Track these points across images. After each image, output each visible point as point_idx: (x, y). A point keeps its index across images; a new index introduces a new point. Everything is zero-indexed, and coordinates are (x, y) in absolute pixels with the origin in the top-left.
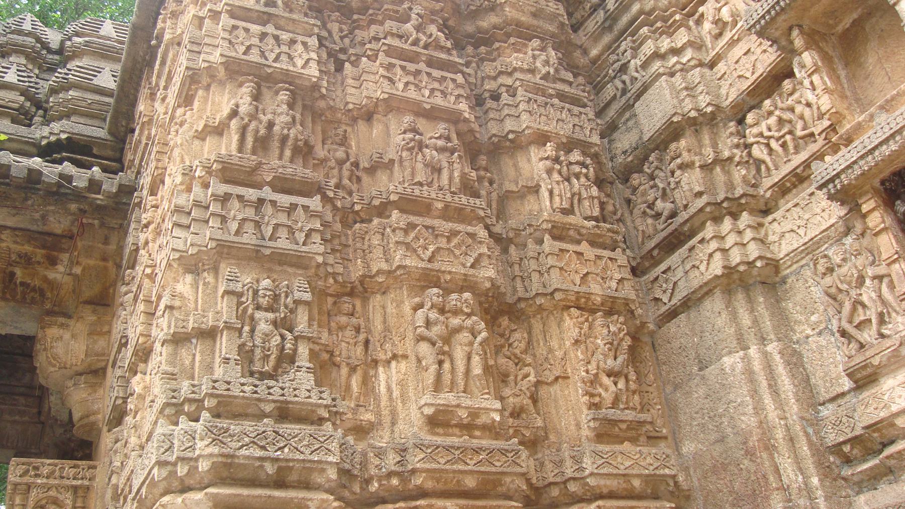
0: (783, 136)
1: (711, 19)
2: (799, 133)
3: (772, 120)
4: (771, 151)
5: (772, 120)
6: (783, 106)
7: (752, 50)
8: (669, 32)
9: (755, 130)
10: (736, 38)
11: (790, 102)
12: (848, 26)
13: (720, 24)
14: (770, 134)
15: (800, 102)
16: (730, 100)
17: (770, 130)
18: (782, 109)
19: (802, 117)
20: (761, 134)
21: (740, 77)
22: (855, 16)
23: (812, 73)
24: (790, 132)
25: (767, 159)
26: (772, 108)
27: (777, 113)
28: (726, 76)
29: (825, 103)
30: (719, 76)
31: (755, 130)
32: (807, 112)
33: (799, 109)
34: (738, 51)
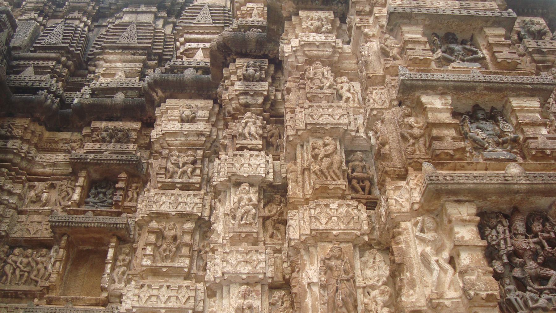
0: (25, 272)
1: (37, 192)
2: (32, 276)
3: (25, 260)
4: (14, 272)
5: (25, 260)
6: (35, 258)
7: (42, 223)
8: (15, 180)
9: (14, 258)
10: (40, 211)
11: (39, 259)
12: (84, 249)
13: (38, 199)
14: (20, 266)
15: (43, 264)
16: (15, 236)
17: (21, 263)
18: (33, 259)
19: (39, 270)
20: (16, 262)
21: (27, 229)
22: (90, 248)
23: (58, 261)
24: (29, 272)
25: (10, 276)
26: (30, 255)
27: (30, 259)
28: (22, 223)
29: (54, 277)
30: (19, 220)
31: (14, 258)
32: (43, 270)
33: (40, 266)
34: (36, 218)
